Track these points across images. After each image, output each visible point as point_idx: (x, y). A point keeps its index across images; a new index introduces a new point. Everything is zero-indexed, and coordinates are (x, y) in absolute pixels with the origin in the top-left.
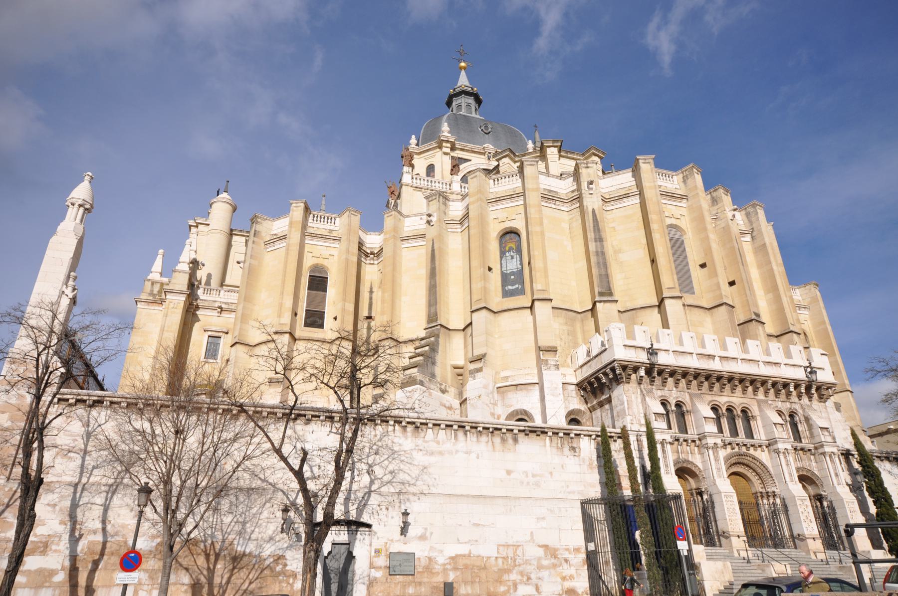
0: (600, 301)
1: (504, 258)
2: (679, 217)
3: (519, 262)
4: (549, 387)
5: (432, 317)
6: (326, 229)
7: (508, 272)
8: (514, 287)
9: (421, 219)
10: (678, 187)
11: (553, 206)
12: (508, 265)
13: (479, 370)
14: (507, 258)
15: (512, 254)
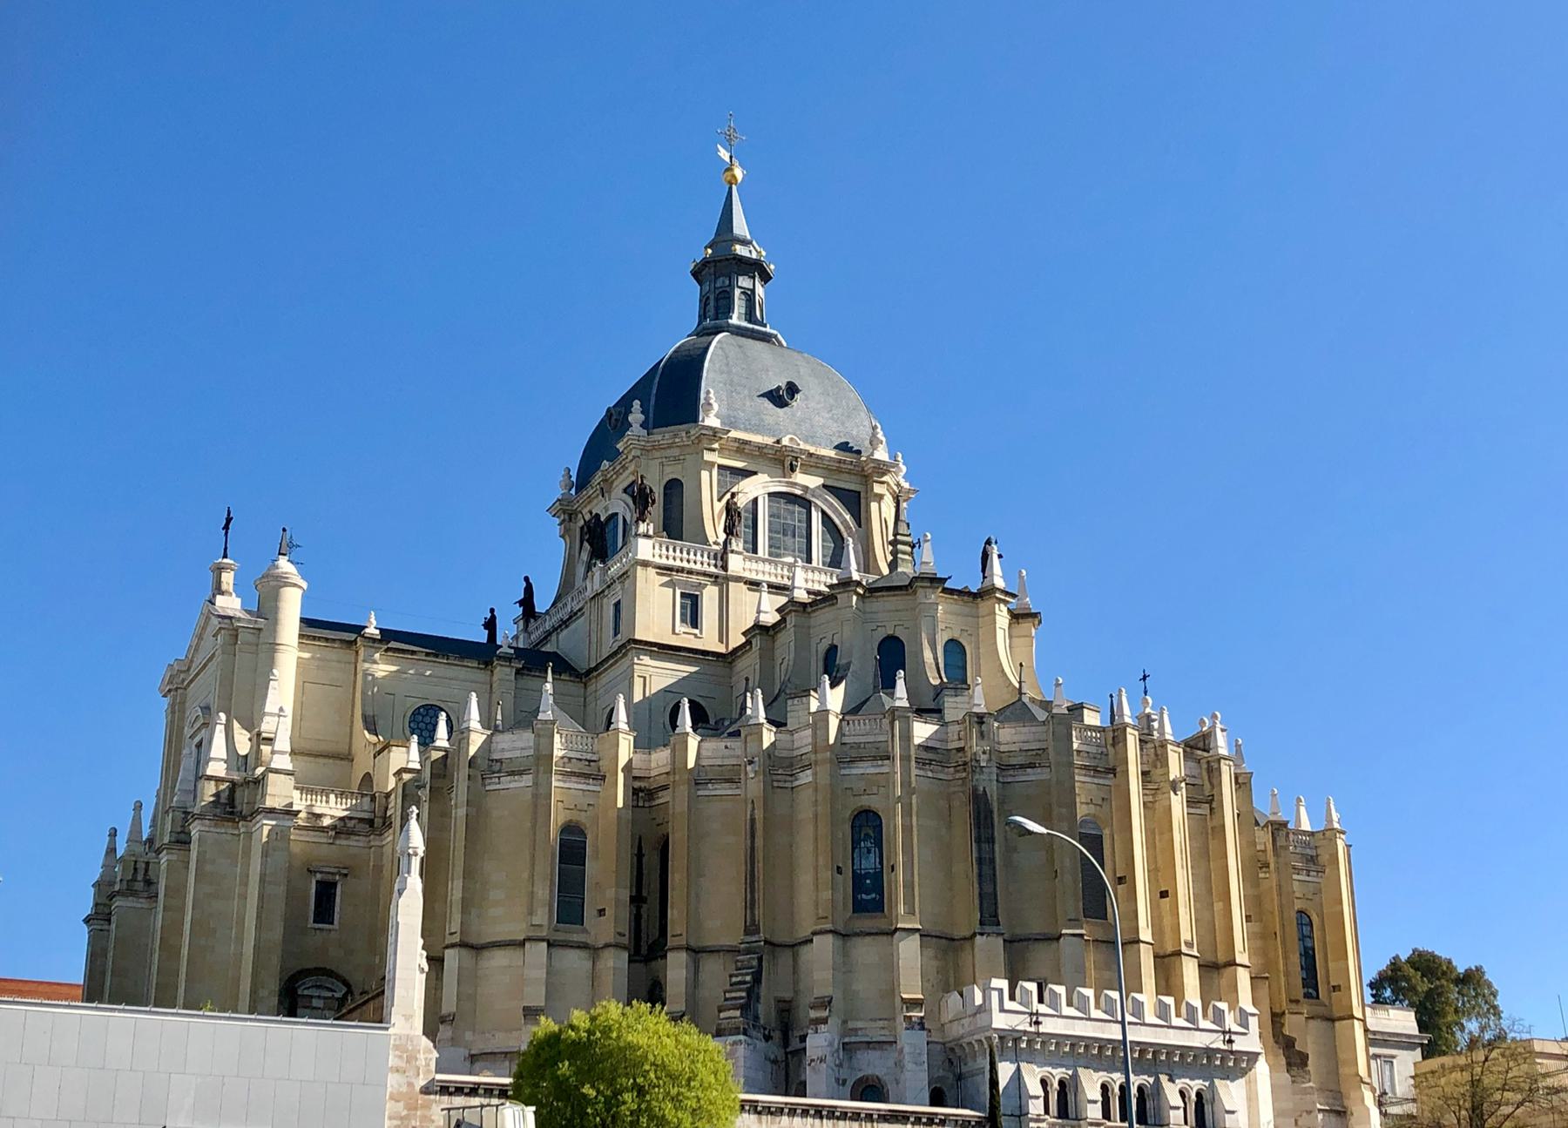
0: (982, 934)
1: (857, 850)
2: (1100, 803)
3: (878, 860)
4: (910, 1053)
5: (751, 928)
6: (580, 760)
7: (863, 872)
8: (869, 897)
9: (726, 747)
10: (1104, 750)
11: (930, 774)
12: (863, 862)
13: (824, 1021)
14: (862, 850)
15: (869, 845)
